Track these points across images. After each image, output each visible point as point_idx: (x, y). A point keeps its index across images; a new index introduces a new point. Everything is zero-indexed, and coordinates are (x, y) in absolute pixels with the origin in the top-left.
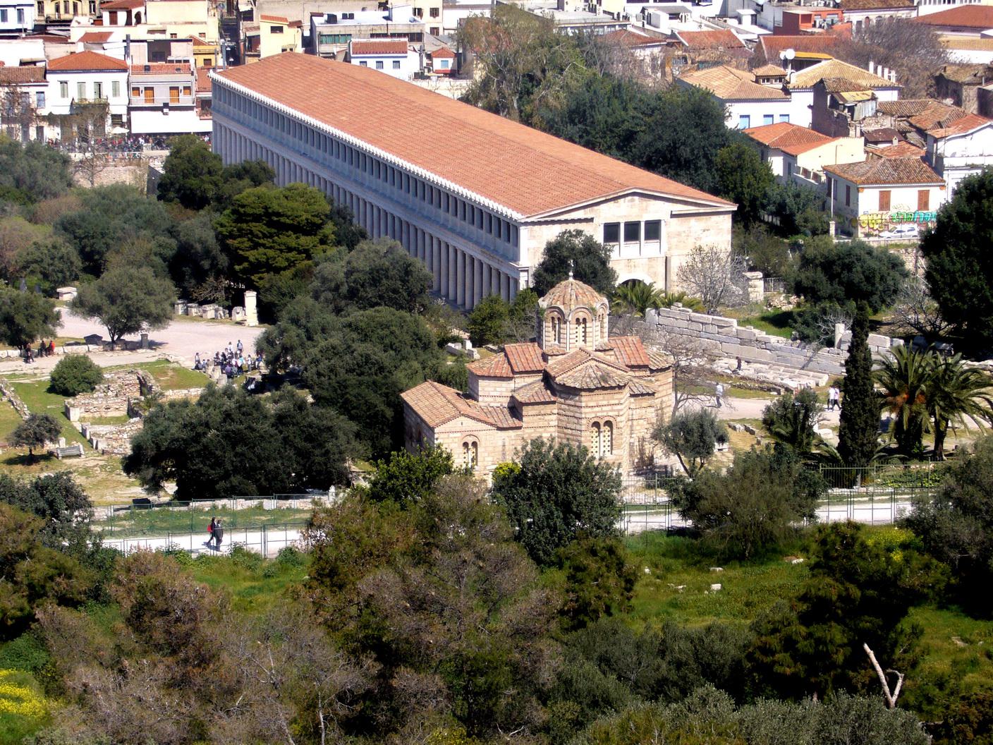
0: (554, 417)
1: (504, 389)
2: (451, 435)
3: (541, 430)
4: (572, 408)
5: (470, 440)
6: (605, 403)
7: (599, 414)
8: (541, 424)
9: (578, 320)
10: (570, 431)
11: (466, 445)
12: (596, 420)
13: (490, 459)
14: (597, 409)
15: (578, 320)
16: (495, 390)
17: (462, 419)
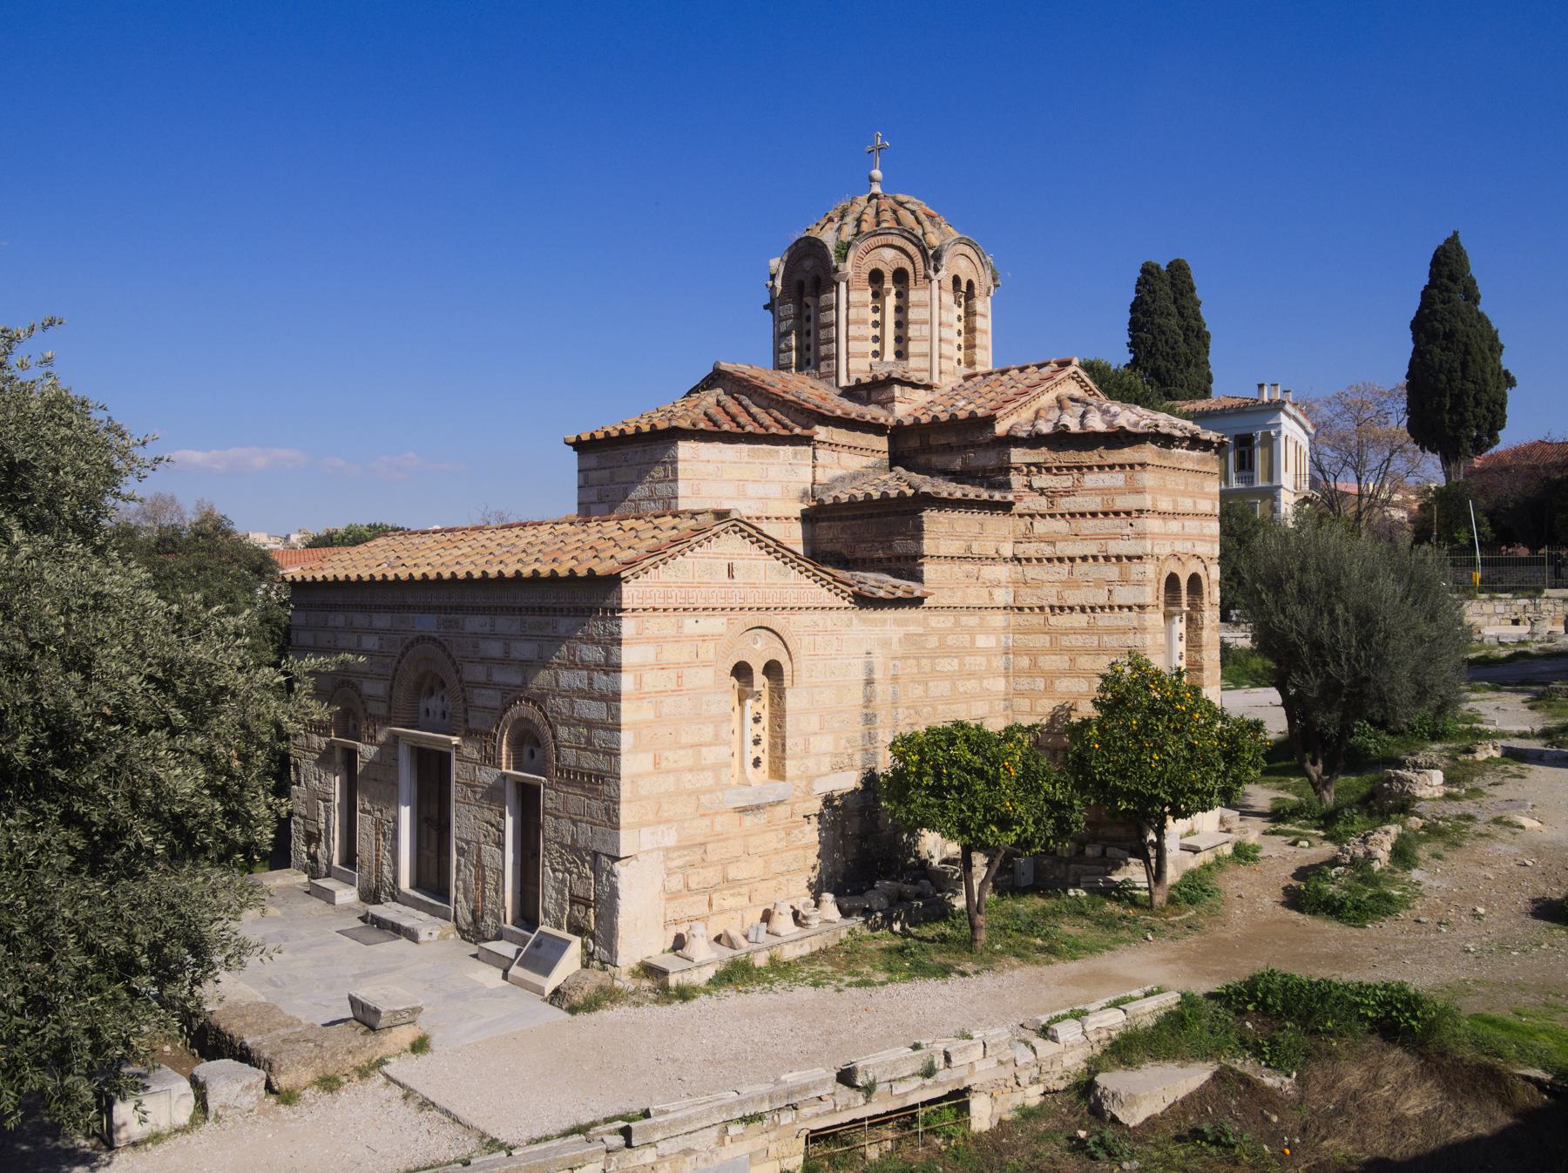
0: (1002, 572)
1: (774, 490)
2: (689, 623)
3: (971, 620)
4: (1088, 525)
5: (758, 653)
6: (1186, 504)
7: (1180, 547)
8: (976, 596)
9: (956, 281)
10: (1079, 620)
11: (741, 671)
12: (1172, 566)
13: (823, 744)
14: (1174, 526)
15: (956, 281)
16: (742, 495)
17: (731, 546)
